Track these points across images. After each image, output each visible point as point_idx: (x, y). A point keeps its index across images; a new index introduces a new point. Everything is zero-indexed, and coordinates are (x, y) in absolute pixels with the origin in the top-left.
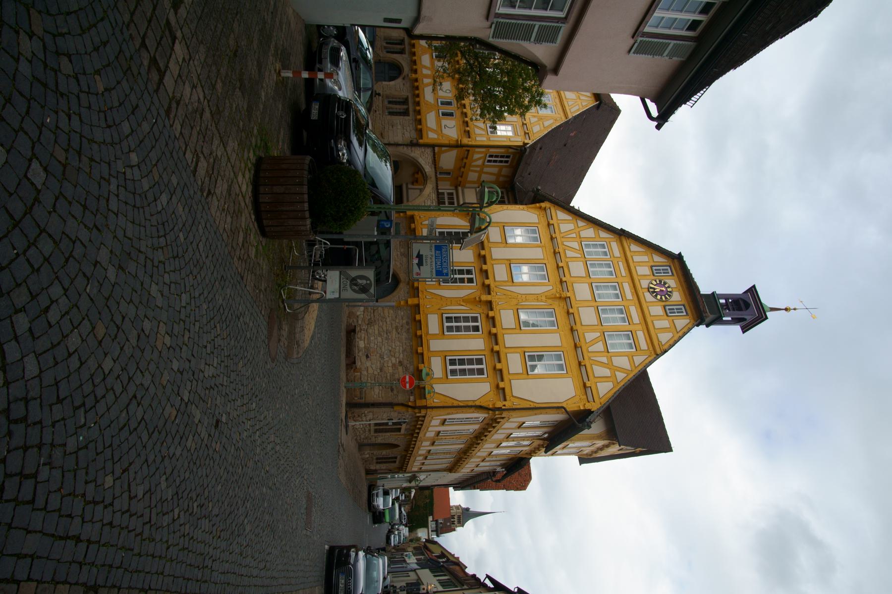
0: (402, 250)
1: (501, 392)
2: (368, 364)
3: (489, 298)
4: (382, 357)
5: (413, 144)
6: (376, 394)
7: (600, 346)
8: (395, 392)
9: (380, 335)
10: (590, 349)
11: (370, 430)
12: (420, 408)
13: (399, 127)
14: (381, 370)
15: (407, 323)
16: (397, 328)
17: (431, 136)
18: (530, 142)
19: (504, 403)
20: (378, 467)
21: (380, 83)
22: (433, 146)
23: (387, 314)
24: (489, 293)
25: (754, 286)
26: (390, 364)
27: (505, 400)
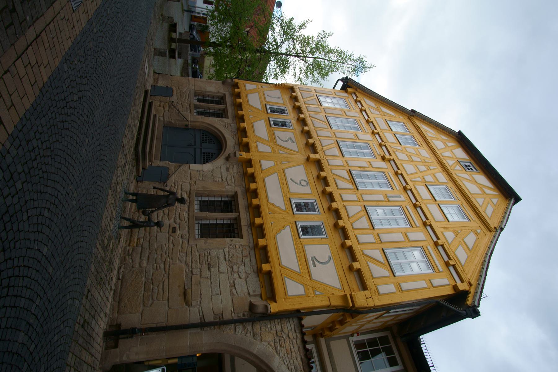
5: (255, 316)
13: (224, 267)
17: (293, 292)
21: (185, 167)
22: (297, 315)
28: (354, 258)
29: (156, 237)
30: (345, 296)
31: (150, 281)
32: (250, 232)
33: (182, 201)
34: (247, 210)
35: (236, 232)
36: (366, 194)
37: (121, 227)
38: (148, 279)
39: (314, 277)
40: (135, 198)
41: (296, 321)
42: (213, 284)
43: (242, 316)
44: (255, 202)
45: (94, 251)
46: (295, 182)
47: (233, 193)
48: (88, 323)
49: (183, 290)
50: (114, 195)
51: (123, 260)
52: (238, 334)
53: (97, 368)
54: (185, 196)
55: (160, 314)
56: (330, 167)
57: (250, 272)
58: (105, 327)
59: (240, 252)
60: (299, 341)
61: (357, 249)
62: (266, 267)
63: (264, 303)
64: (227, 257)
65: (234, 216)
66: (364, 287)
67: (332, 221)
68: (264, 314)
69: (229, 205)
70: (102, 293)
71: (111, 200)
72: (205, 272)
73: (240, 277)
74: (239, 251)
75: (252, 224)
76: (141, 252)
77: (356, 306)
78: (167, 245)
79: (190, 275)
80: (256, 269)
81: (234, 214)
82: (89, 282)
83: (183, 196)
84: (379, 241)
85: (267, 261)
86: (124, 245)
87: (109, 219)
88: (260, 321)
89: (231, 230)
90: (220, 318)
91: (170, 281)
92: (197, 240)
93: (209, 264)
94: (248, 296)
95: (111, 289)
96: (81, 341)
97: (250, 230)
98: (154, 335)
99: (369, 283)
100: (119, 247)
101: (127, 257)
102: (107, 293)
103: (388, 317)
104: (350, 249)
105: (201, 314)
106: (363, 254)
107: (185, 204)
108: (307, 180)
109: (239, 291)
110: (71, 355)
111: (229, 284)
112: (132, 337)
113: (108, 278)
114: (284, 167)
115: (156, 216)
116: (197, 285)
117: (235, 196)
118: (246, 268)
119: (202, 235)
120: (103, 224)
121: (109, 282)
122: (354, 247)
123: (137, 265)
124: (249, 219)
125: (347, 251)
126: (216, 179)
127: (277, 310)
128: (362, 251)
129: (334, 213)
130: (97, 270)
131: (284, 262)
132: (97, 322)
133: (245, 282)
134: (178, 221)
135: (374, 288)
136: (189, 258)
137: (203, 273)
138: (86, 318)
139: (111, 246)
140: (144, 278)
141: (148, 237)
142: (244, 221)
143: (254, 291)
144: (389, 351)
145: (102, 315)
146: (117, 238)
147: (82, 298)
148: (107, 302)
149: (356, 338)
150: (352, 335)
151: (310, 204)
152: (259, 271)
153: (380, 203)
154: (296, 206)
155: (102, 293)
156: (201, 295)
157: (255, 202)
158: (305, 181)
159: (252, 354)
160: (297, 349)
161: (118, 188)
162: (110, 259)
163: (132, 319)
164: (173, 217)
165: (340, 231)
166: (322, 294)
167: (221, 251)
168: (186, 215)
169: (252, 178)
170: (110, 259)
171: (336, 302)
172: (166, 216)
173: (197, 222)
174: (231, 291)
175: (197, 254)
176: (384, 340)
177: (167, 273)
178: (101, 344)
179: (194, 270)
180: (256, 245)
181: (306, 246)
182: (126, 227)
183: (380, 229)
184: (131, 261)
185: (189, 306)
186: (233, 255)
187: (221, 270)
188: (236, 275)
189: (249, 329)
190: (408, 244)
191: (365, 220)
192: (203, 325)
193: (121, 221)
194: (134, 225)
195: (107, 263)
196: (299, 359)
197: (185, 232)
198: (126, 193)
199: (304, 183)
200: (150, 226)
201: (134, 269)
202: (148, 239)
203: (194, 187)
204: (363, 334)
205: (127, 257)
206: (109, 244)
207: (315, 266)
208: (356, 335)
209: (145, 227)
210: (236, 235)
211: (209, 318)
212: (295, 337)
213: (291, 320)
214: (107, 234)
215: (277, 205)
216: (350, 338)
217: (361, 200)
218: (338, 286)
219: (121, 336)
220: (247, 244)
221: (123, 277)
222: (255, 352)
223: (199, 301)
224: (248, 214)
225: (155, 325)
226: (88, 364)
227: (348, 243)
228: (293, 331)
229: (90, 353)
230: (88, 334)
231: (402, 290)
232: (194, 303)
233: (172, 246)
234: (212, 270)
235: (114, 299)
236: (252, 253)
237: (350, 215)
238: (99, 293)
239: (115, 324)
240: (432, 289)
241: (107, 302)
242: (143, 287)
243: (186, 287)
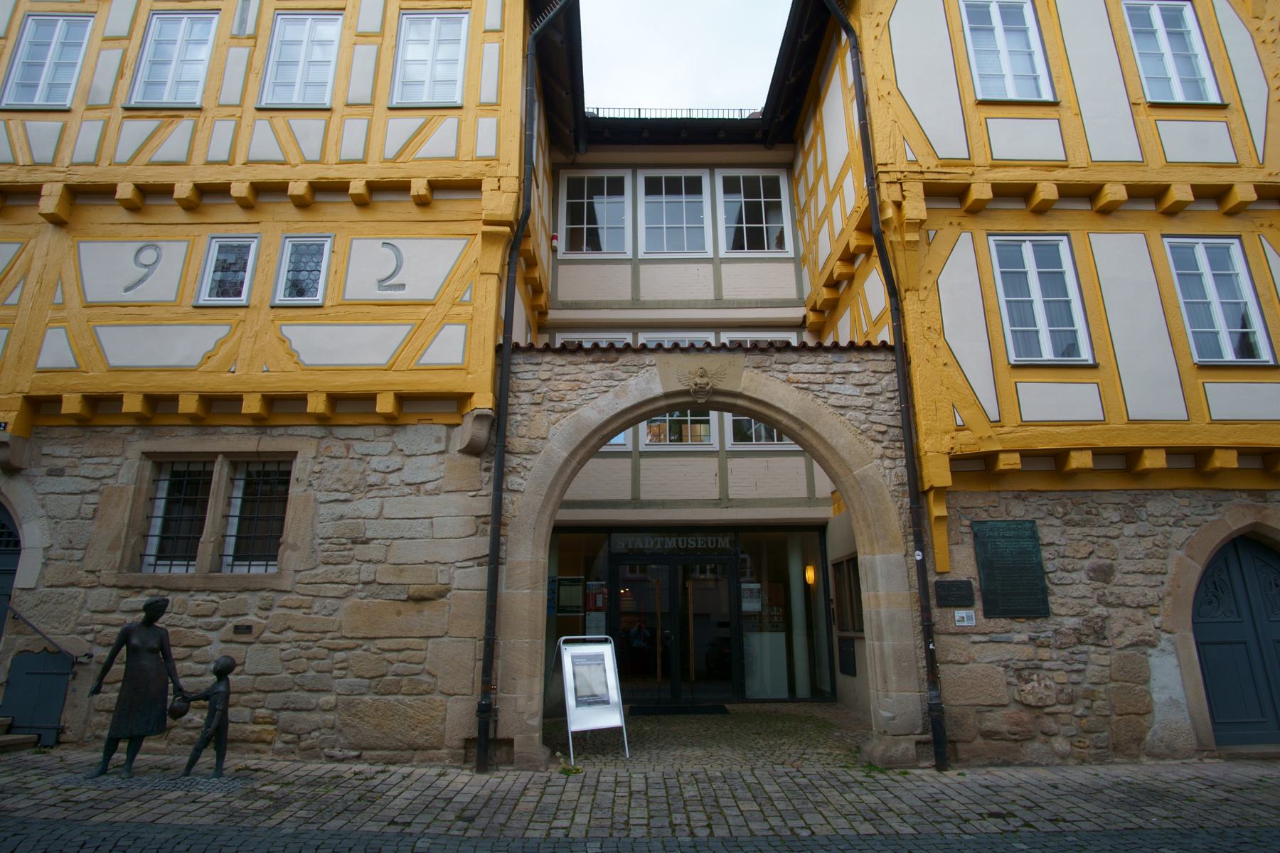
5: (493, 447)
13: (366, 506)
17: (456, 353)
21: (22, 603)
22: (505, 353)
28: (401, 187)
29: (257, 675)
30: (485, 235)
31: (374, 683)
32: (281, 430)
33: (155, 610)
34: (211, 430)
35: (273, 468)
36: (219, 90)
37: (219, 770)
38: (369, 687)
39: (429, 295)
40: (123, 745)
41: (518, 359)
42: (406, 535)
43: (488, 474)
44: (188, 405)
45: (288, 829)
46: (141, 281)
47: (149, 465)
48: (463, 810)
49: (410, 605)
50: (109, 805)
51: (312, 753)
52: (525, 485)
53: (547, 774)
54: (140, 600)
55: (455, 656)
56: (104, 164)
57: (390, 444)
58: (467, 772)
59: (335, 462)
60: (559, 360)
61: (377, 171)
62: (385, 405)
63: (468, 421)
64: (343, 496)
65: (226, 469)
66: (474, 186)
67: (289, 211)
68: (492, 426)
69: (186, 483)
70: (393, 792)
71: (128, 812)
72: (373, 551)
73: (399, 469)
74: (330, 464)
75: (259, 423)
76: (295, 710)
77: (511, 218)
78: (283, 646)
79: (374, 587)
80: (385, 430)
81: (217, 468)
82: (373, 827)
83: (141, 607)
84: (368, 110)
85: (370, 398)
86: (269, 755)
87: (203, 803)
88: (506, 437)
89: (267, 483)
90: (484, 523)
91: (383, 635)
92: (281, 570)
93: (354, 542)
94: (446, 456)
95: (383, 772)
96: (501, 818)
97: (276, 432)
98: (499, 664)
99: (466, 172)
100: (275, 767)
101: (303, 744)
102: (393, 779)
103: (541, 162)
104: (374, 187)
105: (470, 563)
106: (394, 160)
107: (167, 601)
108: (141, 245)
109: (431, 476)
110: (529, 834)
111: (412, 497)
112: (496, 710)
113: (357, 783)
114: (76, 303)
115: (192, 679)
116: (401, 571)
117: (159, 461)
118: (378, 451)
119: (270, 554)
120: (209, 820)
121: (367, 779)
122: (373, 177)
123: (330, 717)
124: (240, 430)
125: (377, 198)
126: (88, 510)
127: (490, 396)
128: (386, 160)
129: (262, 199)
130: (338, 814)
131: (381, 359)
132: (459, 792)
133: (413, 459)
134: (216, 619)
135: (480, 166)
136: (330, 590)
137: (374, 557)
138: (452, 817)
139: (272, 788)
140: (366, 698)
141: (255, 696)
142: (248, 443)
143: (438, 440)
144: (596, 188)
145: (442, 782)
146: (247, 777)
147: (411, 834)
148: (415, 777)
149: (561, 244)
150: (554, 250)
151: (222, 257)
152: (391, 422)
153: (257, 63)
154: (223, 293)
155: (393, 792)
156: (426, 562)
157: (188, 405)
158: (140, 251)
159: (567, 462)
160: (573, 367)
161: (83, 798)
162: (309, 784)
163: (458, 715)
164: (201, 632)
165: (319, 198)
166: (470, 287)
167: (323, 509)
168: (201, 597)
169: (101, 405)
170: (309, 784)
171: (495, 259)
172: (196, 652)
173: (226, 571)
174: (428, 493)
175: (322, 569)
176: (575, 189)
177: (360, 642)
178: (502, 774)
179: (364, 577)
180: (322, 421)
181: (347, 297)
182: (221, 757)
183: (334, 94)
184: (316, 734)
185: (449, 590)
186: (339, 480)
187: (375, 513)
188: (393, 479)
189: (519, 461)
190: (389, 41)
191: (300, 124)
192: (494, 561)
193: (197, 774)
194: (217, 736)
195: (321, 790)
196: (592, 367)
197: (253, 600)
198: (104, 771)
199: (148, 256)
200: (228, 693)
201: (338, 723)
202: (261, 696)
203: (108, 575)
204: (555, 228)
205: (303, 744)
206: (269, 796)
207: (402, 286)
208: (555, 243)
209: (227, 705)
210: (283, 468)
211: (482, 545)
212: (550, 367)
213: (514, 369)
214: (238, 804)
215: (210, 346)
216: (560, 256)
217: (238, 112)
218: (460, 244)
219: (491, 736)
220: (315, 442)
221: (354, 749)
222: (565, 455)
223: (442, 568)
224: (225, 430)
225: (480, 664)
226: (543, 794)
227: (357, 187)
228: (536, 368)
229: (522, 794)
230: (485, 805)
231: (496, 104)
232: (443, 579)
233: (290, 635)
234: (369, 534)
235: (408, 761)
236: (341, 432)
237: (280, 157)
238: (395, 797)
239: (462, 751)
240: (505, 36)
241: (415, 777)
242: (389, 697)
243: (404, 597)
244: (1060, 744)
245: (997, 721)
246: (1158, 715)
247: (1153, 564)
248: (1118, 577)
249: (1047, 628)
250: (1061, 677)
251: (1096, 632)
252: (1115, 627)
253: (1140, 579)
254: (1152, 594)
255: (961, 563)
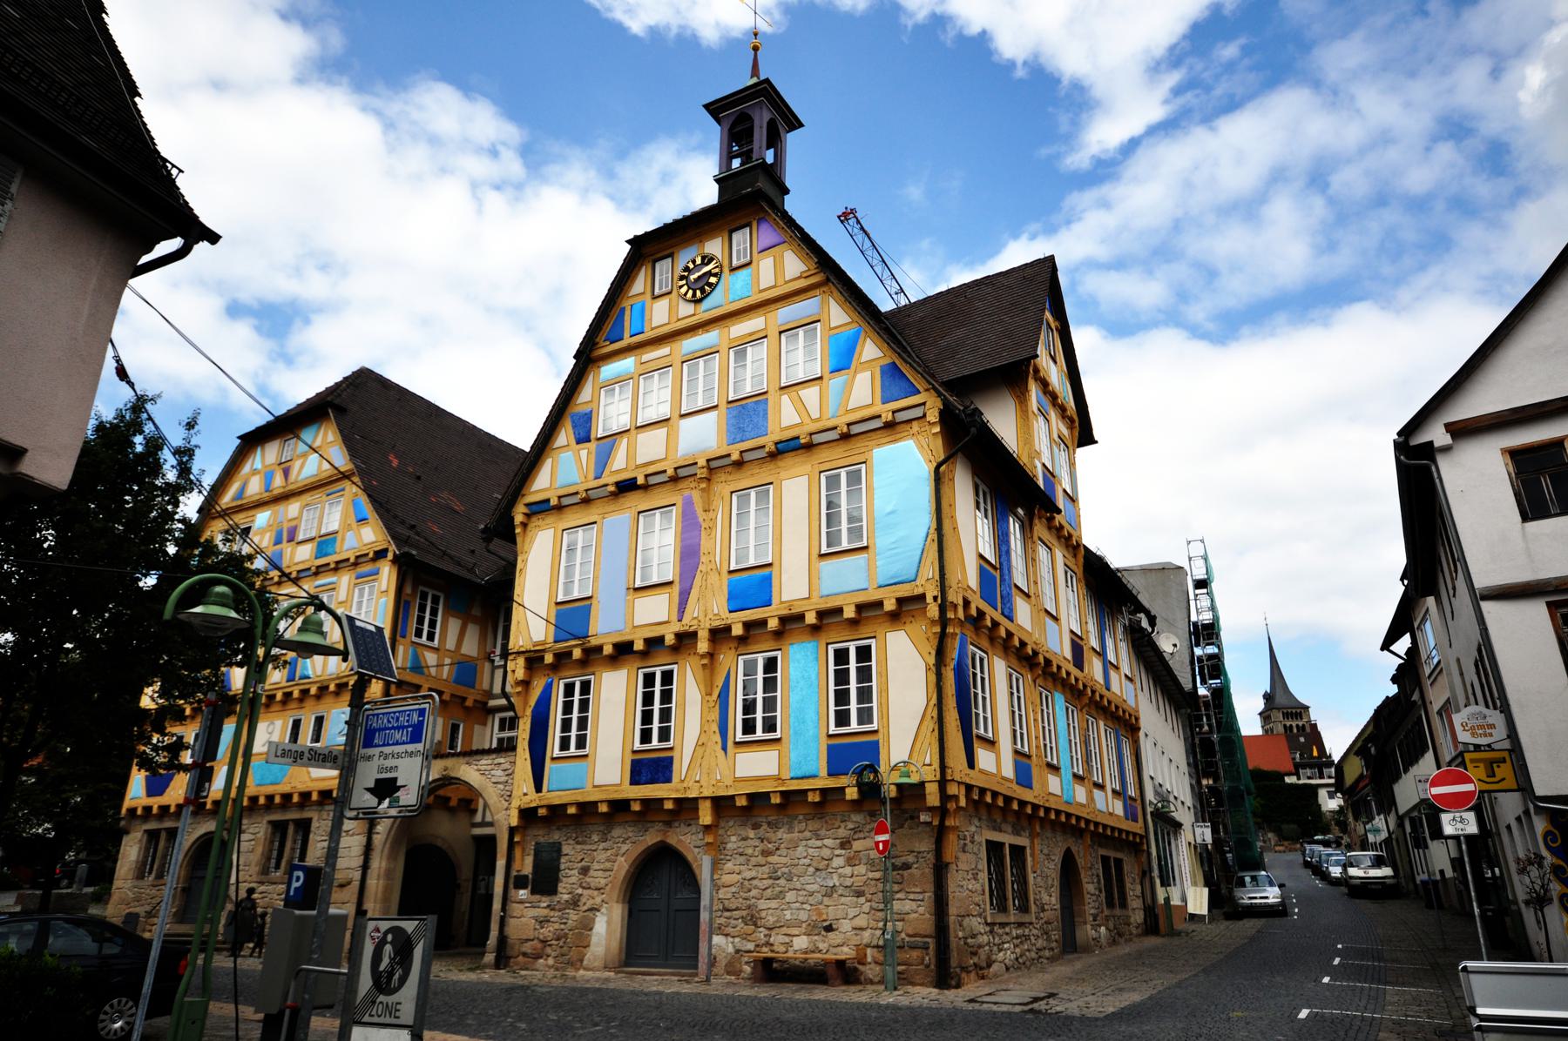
0: (595, 838)
1: (907, 608)
2: (846, 926)
3: (703, 635)
4: (830, 892)
6: (914, 909)
7: (810, 395)
8: (911, 859)
9: (780, 895)
10: (815, 414)
11: (1020, 925)
12: (945, 797)
14: (859, 894)
15: (756, 827)
16: (766, 853)
18: (393, 548)
19: (929, 599)
20: (1135, 903)
23: (735, 878)
24: (694, 635)
25: (706, 107)
26: (848, 870)
27: (922, 597)
244: (551, 961)
245: (527, 948)
246: (592, 948)
247: (608, 865)
248: (592, 873)
249: (556, 899)
250: (557, 926)
251: (575, 903)
252: (583, 900)
253: (600, 873)
254: (603, 881)
255: (526, 865)
